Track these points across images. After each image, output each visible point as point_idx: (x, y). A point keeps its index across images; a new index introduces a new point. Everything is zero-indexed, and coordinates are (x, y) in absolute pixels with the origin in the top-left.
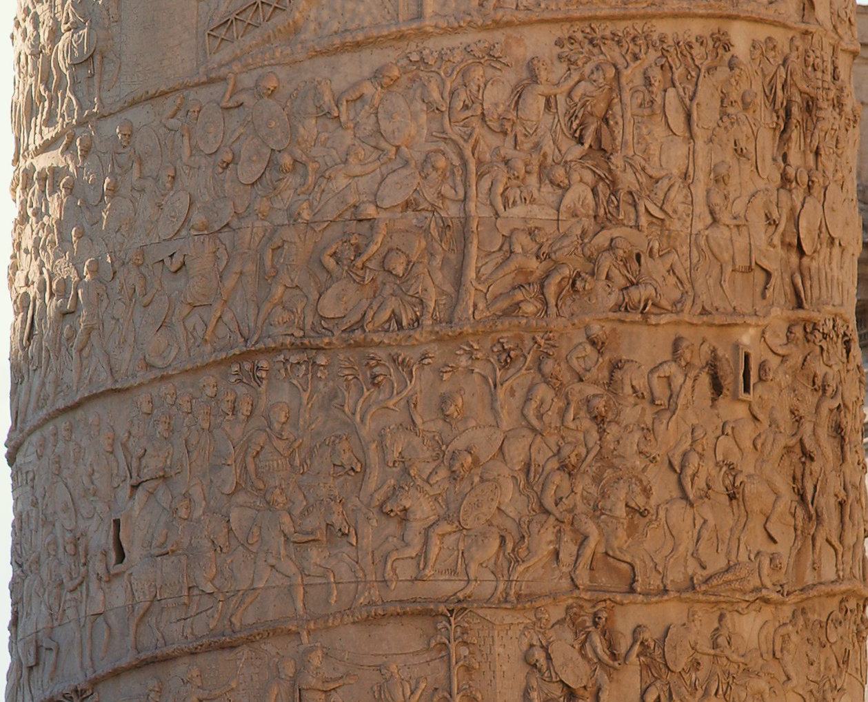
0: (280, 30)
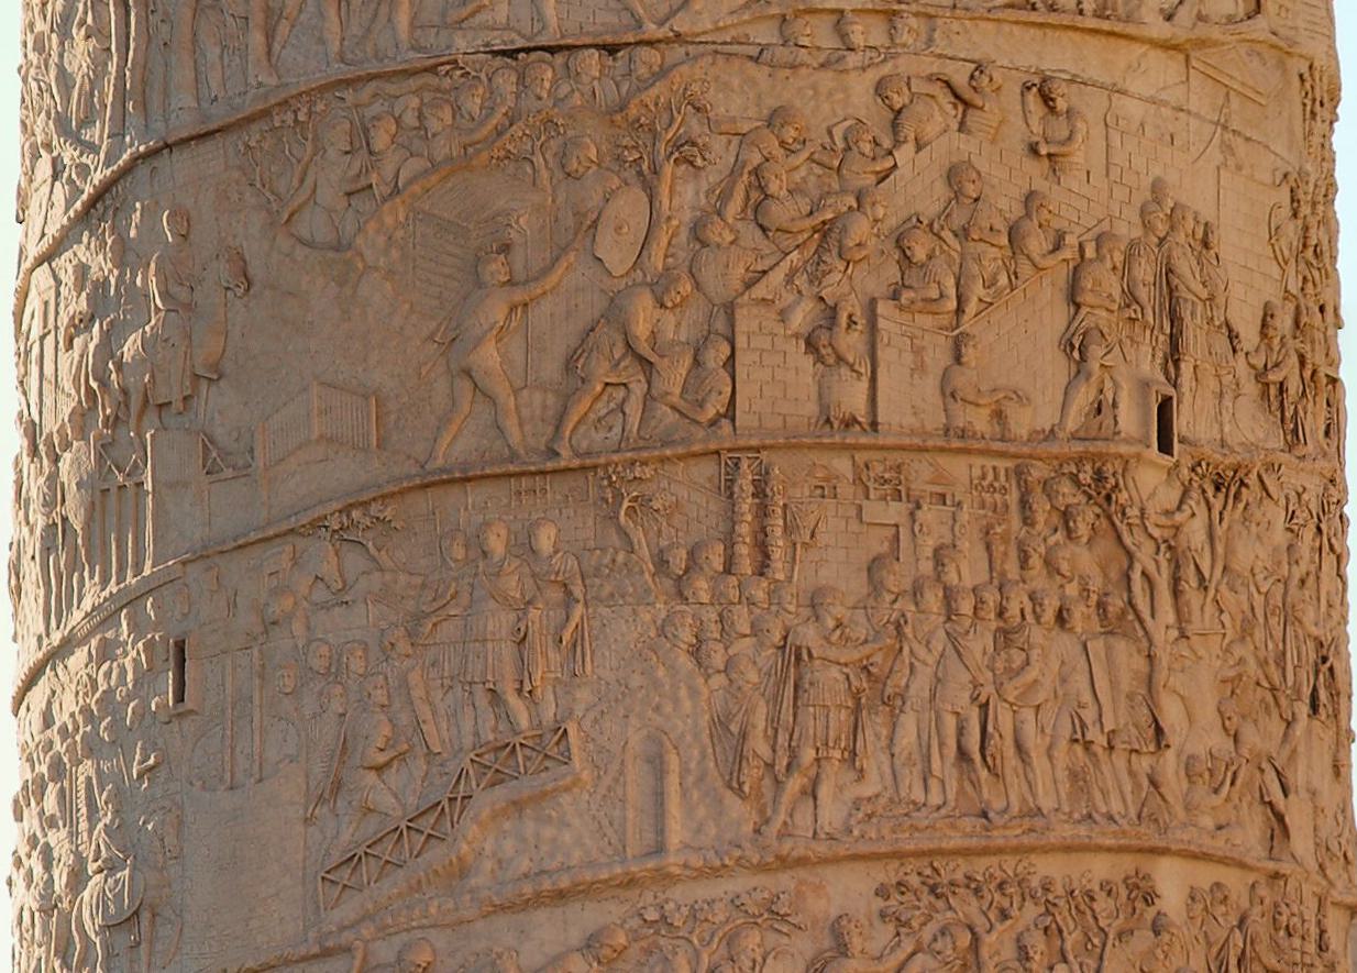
0: (436, 872)
